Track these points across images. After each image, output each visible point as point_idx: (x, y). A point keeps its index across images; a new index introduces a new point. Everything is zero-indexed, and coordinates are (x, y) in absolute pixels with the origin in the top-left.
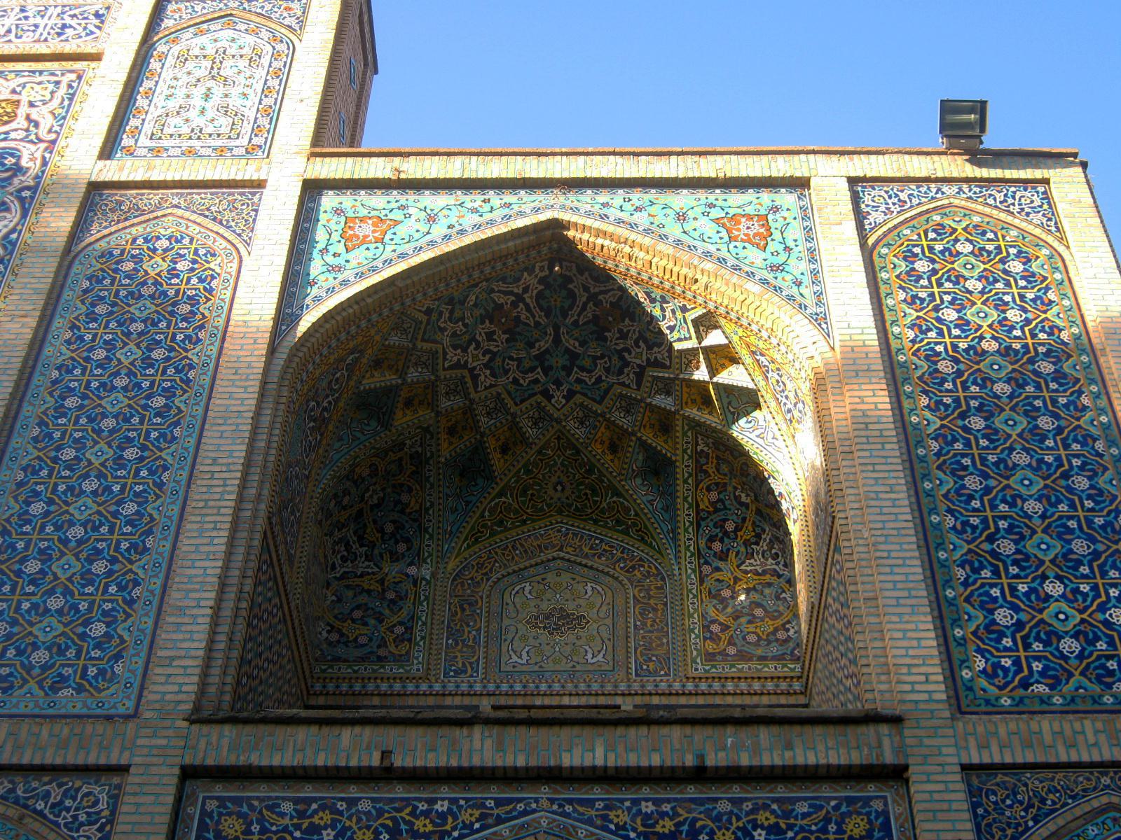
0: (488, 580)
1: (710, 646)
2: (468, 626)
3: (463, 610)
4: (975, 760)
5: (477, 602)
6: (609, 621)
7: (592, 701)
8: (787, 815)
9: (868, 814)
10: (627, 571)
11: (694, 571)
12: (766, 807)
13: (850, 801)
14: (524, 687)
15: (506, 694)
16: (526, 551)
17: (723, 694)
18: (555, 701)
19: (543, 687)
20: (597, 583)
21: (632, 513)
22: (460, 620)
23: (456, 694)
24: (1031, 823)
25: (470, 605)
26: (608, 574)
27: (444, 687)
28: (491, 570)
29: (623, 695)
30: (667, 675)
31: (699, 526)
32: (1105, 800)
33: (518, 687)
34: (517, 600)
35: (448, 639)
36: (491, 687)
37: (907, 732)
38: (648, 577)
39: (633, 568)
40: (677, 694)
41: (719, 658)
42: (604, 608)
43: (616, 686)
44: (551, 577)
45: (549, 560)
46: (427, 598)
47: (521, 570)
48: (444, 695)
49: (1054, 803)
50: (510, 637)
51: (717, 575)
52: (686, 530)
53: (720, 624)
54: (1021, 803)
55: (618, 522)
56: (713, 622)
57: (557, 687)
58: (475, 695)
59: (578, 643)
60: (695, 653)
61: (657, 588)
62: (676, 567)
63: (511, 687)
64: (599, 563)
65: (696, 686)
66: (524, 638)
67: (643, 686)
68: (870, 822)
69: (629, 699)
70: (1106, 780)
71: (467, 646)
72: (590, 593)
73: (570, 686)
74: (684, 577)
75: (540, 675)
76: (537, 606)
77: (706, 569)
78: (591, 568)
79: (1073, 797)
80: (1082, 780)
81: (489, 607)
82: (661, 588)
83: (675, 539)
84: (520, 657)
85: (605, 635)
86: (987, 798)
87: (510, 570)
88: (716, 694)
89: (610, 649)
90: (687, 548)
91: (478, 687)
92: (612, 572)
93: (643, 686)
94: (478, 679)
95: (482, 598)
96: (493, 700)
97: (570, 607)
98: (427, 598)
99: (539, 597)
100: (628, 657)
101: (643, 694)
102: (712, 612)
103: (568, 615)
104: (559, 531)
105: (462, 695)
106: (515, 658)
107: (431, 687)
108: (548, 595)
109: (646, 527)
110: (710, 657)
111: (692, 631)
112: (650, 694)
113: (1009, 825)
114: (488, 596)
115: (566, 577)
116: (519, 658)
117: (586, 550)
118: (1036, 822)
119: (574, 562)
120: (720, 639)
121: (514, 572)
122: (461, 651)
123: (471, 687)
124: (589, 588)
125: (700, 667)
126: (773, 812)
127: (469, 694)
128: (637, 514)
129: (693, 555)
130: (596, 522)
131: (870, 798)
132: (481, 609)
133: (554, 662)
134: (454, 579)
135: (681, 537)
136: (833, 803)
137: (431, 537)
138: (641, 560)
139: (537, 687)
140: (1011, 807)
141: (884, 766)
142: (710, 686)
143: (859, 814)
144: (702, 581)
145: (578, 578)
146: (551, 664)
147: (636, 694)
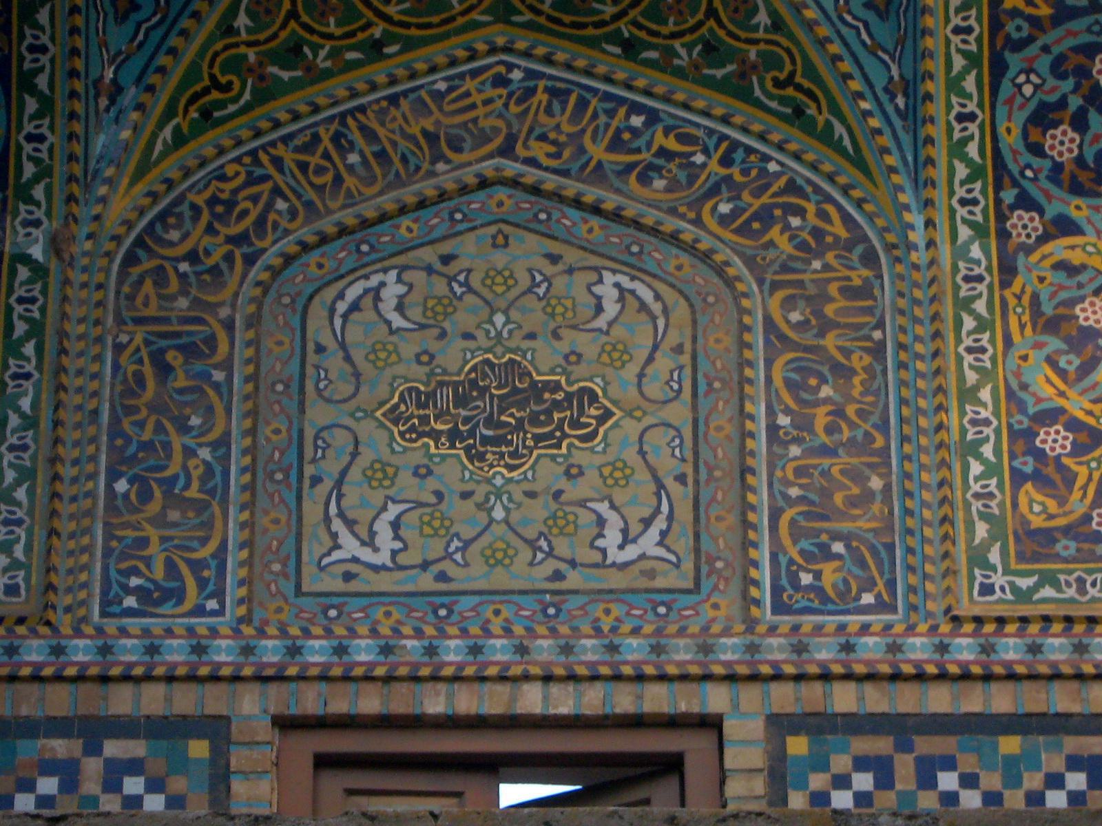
0: (250, 260)
1: (1036, 506)
2: (184, 429)
3: (164, 370)
5: (211, 341)
6: (679, 413)
7: (624, 701)
10: (743, 231)
11: (980, 231)
14: (386, 650)
15: (324, 678)
16: (382, 156)
17: (1080, 677)
18: (490, 701)
19: (453, 651)
20: (638, 271)
21: (763, 18)
22: (153, 408)
23: (148, 678)
25: (190, 351)
26: (673, 237)
27: (105, 650)
28: (261, 222)
29: (731, 678)
30: (882, 606)
31: (998, 68)
33: (363, 652)
34: (354, 334)
35: (113, 476)
36: (271, 651)
38: (820, 255)
39: (765, 217)
40: (920, 677)
41: (1066, 547)
42: (664, 363)
43: (706, 649)
44: (469, 248)
45: (464, 190)
46: (36, 330)
47: (365, 224)
48: (104, 679)
50: (331, 468)
51: (1059, 248)
52: (954, 85)
53: (1074, 425)
55: (711, 49)
56: (1050, 416)
57: (499, 650)
58: (215, 678)
59: (574, 491)
60: (981, 530)
61: (850, 292)
62: (916, 218)
63: (341, 650)
64: (646, 200)
65: (987, 649)
66: (381, 473)
67: (800, 649)
69: (750, 695)
71: (184, 503)
72: (611, 309)
73: (544, 649)
74: (945, 253)
75: (441, 604)
76: (425, 357)
77: (1024, 224)
78: (616, 216)
81: (255, 361)
82: (864, 291)
83: (914, 117)
84: (369, 542)
85: (667, 465)
87: (327, 225)
88: (1056, 676)
89: (684, 513)
90: (957, 149)
91: (224, 653)
92: (689, 232)
93: (800, 649)
94: (223, 623)
95: (229, 326)
96: (277, 699)
97: (543, 362)
98: (36, 330)
99: (433, 323)
100: (748, 544)
101: (799, 678)
102: (1043, 385)
103: (537, 390)
104: (501, 81)
105: (170, 679)
106: (350, 546)
107: (58, 651)
108: (464, 318)
109: (811, 71)
110: (1035, 545)
111: (973, 449)
112: (825, 677)
114: (253, 321)
115: (527, 250)
116: (364, 543)
117: (597, 151)
119: (557, 196)
120: (1069, 479)
121: (343, 231)
122: (159, 521)
123: (199, 650)
124: (607, 291)
125: (998, 580)
127: (192, 678)
128: (777, 25)
129: (976, 173)
130: (630, 48)
132: (227, 366)
133: (493, 560)
134: (131, 259)
135: (936, 109)
137: (46, 106)
138: (792, 187)
139: (431, 651)
142: (1035, 649)
144: (1008, 271)
145: (572, 256)
146: (478, 568)
147: (777, 677)
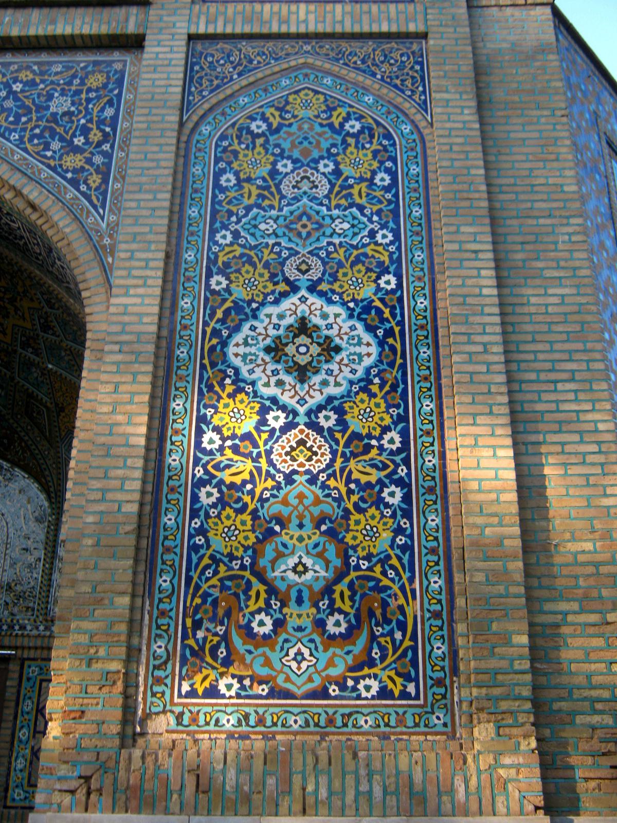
4: (202, 30)
8: (42, 73)
9: (108, 73)
12: (28, 68)
13: (96, 63)
24: (235, 77)
32: (301, 61)
37: (151, 12)
49: (259, 62)
54: (232, 63)
68: (108, 78)
70: (307, 48)
79: (276, 59)
80: (288, 46)
86: (206, 58)
113: (217, 78)
118: (240, 75)
126: (33, 72)
131: (113, 62)
136: (82, 65)
140: (223, 65)
141: (127, 36)
143: (100, 72)
